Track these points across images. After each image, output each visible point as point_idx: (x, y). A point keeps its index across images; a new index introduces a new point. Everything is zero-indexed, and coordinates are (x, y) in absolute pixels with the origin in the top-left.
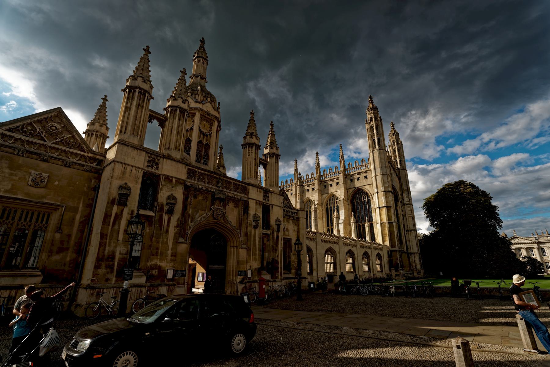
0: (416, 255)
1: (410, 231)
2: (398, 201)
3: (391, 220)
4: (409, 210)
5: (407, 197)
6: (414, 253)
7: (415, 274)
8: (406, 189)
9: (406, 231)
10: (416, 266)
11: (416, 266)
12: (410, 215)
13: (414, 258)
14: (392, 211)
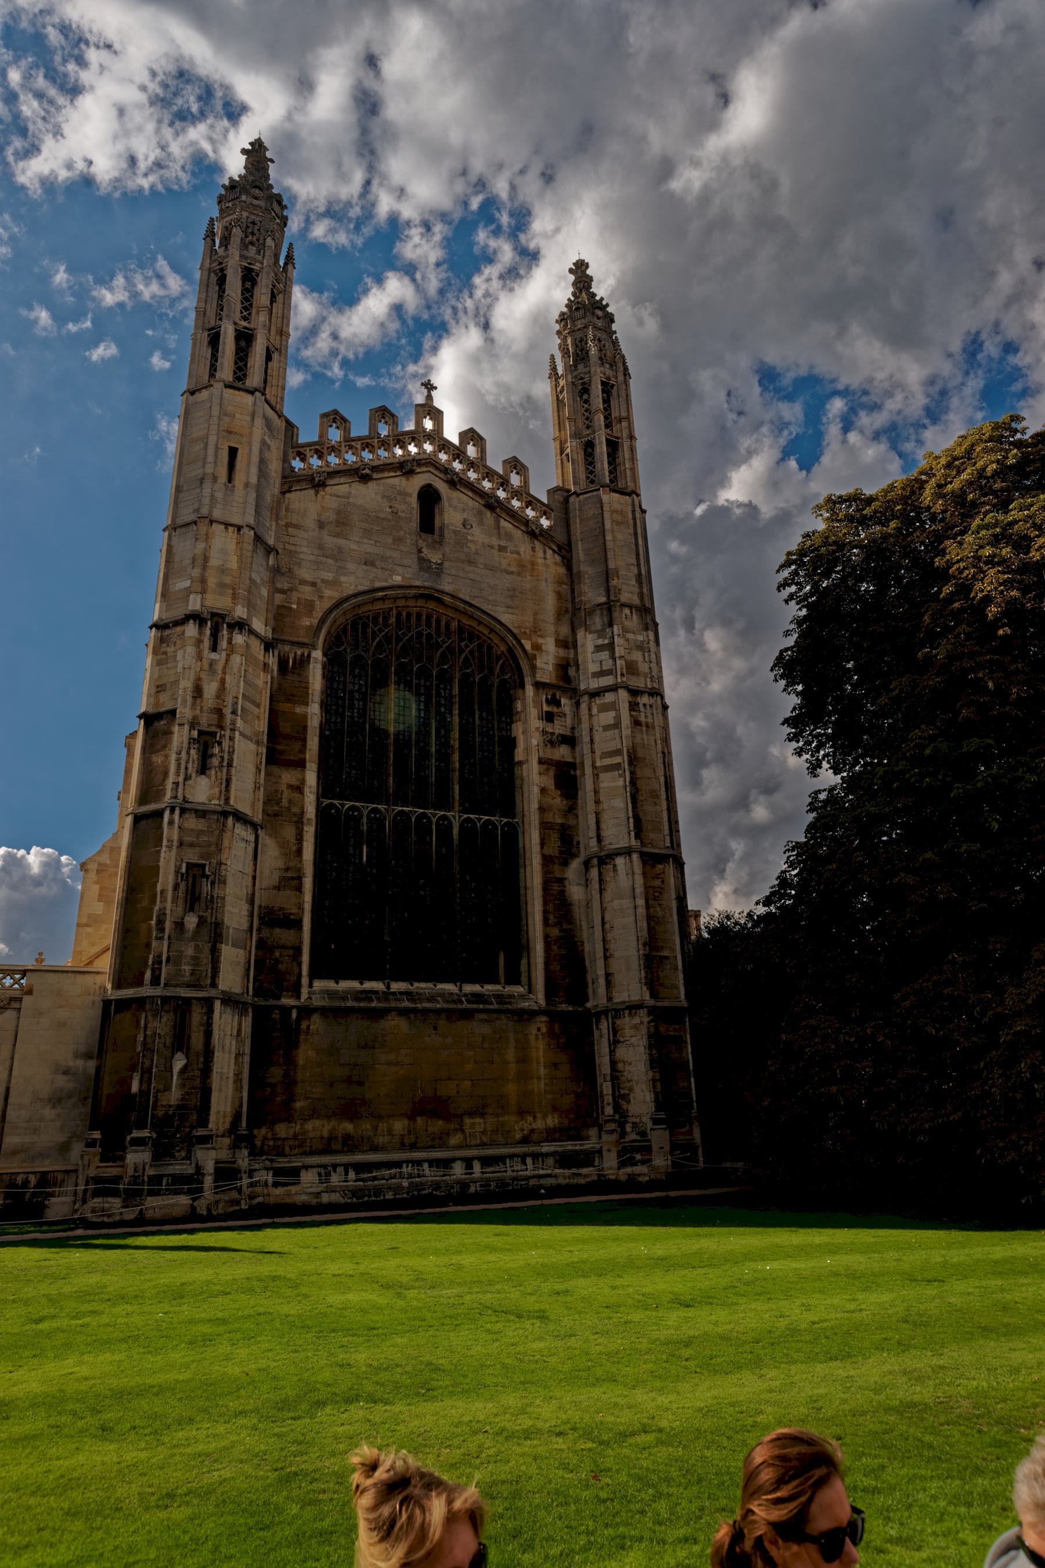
0: (626, 1022)
2: (522, 686)
3: (159, 795)
4: (607, 728)
5: (598, 649)
6: (616, 1012)
7: (610, 1164)
8: (603, 599)
9: (587, 864)
10: (620, 1098)
11: (626, 1098)
13: (614, 1044)
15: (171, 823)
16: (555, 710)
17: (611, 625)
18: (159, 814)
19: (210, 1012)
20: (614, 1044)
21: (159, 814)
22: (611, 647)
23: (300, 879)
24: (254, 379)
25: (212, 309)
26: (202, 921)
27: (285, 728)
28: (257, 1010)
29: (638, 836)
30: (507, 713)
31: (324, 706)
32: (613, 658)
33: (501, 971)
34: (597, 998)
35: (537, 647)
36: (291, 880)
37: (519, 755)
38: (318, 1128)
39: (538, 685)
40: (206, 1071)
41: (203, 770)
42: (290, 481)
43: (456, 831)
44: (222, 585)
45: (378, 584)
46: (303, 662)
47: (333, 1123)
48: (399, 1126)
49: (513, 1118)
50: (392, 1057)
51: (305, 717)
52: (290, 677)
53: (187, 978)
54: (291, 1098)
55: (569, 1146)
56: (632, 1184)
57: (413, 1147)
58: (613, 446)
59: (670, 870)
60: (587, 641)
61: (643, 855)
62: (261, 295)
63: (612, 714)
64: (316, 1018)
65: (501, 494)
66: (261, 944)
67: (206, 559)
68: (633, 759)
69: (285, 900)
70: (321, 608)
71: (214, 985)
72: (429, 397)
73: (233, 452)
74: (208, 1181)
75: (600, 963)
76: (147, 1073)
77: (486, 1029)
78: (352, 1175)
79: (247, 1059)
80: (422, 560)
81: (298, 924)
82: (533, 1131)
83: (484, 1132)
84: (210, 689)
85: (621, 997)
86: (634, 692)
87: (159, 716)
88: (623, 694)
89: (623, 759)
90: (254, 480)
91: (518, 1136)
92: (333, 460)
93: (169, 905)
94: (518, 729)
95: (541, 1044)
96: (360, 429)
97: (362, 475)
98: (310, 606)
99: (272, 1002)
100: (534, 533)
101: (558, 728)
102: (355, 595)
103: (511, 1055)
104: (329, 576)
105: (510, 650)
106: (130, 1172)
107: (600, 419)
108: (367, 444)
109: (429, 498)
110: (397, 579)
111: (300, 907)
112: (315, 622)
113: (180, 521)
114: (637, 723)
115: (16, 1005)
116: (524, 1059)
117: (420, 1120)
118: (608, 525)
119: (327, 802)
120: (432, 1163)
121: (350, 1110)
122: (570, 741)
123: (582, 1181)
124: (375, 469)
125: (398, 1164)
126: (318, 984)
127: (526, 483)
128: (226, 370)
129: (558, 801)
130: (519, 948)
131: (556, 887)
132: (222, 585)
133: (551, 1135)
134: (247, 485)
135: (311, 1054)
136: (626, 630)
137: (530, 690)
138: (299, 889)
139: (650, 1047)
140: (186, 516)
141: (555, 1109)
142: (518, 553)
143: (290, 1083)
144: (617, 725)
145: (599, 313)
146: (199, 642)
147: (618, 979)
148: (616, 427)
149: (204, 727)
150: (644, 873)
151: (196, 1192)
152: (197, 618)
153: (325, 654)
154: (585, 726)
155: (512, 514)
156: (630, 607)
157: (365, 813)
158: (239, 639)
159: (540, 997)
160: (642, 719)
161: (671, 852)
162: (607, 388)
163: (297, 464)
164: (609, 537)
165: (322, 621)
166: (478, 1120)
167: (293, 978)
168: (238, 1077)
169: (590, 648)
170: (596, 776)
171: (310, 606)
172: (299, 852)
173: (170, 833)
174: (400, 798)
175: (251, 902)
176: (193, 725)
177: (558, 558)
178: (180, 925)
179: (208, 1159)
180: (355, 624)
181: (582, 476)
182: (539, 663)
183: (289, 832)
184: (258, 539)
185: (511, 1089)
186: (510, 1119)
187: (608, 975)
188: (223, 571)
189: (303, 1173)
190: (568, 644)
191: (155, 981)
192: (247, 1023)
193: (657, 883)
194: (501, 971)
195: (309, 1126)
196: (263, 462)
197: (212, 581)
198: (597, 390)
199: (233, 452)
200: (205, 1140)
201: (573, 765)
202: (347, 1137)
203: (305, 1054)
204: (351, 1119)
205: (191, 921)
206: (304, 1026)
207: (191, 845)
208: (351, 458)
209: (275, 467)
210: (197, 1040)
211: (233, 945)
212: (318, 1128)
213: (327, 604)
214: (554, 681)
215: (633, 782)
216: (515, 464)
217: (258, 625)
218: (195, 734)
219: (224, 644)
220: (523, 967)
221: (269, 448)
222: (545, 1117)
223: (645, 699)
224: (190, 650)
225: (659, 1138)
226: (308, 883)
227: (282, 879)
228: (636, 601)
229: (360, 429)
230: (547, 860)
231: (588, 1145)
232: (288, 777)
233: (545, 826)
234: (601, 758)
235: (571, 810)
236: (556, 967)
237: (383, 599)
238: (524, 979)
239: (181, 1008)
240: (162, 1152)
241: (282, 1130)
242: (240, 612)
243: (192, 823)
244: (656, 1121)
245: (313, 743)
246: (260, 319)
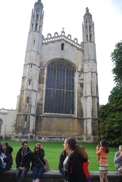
0: (88, 120)
1: (86, 98)
2: (76, 72)
4: (88, 78)
5: (87, 66)
6: (87, 119)
7: (85, 140)
8: (88, 59)
12: (88, 82)
14: (27, 80)
15: (25, 92)
16: (80, 75)
17: (89, 62)
18: (24, 90)
19: (30, 116)
20: (86, 123)
21: (24, 90)
22: (89, 65)
23: (43, 99)
24: (38, 30)
25: (32, 21)
26: (29, 104)
28: (36, 116)
29: (91, 94)
30: (73, 75)
31: (47, 75)
32: (89, 67)
33: (71, 112)
34: (84, 117)
35: (78, 66)
36: (42, 99)
37: (75, 82)
38: (44, 132)
39: (78, 72)
40: (29, 124)
41: (30, 84)
42: (43, 44)
43: (65, 93)
44: (32, 59)
45: (55, 58)
46: (44, 69)
47: (46, 132)
48: (55, 133)
49: (72, 133)
50: (55, 123)
51: (44, 77)
52: (42, 71)
53: (27, 112)
54: (41, 128)
55: (79, 137)
56: (87, 143)
57: (57, 136)
58: (91, 35)
59: (96, 99)
60: (86, 65)
61: (92, 96)
62: (39, 18)
63: (89, 76)
64: (44, 118)
65: (74, 44)
66: (37, 108)
67: (31, 56)
68: (91, 82)
69: (41, 102)
71: (30, 113)
72: (63, 30)
73: (34, 41)
74: (29, 137)
75: (85, 112)
76: (22, 123)
77: (68, 120)
78: (49, 138)
79: (35, 123)
80: (61, 54)
81: (42, 105)
82: (74, 135)
83: (67, 134)
84: (31, 74)
85: (87, 117)
86: (92, 72)
87: (24, 77)
88: (90, 73)
89: (90, 82)
90: (37, 44)
91: (72, 135)
92: (49, 40)
93: (25, 102)
94: (75, 78)
95: (76, 123)
96: (53, 36)
97: (53, 42)
98: (45, 61)
99: (38, 115)
100: (78, 49)
101: (81, 78)
102: (52, 60)
103: (71, 124)
105: (74, 66)
106: (20, 135)
107: (89, 31)
108: (54, 38)
109: (63, 45)
110: (58, 57)
111: (43, 103)
112: (46, 64)
113: (28, 51)
114: (92, 77)
115: (7, 114)
116: (73, 125)
117: (58, 132)
118: (89, 47)
119: (47, 89)
120: (59, 138)
121: (49, 130)
122: (83, 80)
123: (81, 142)
124: (55, 41)
125: (55, 138)
126: (45, 113)
127: (77, 41)
128: (34, 30)
129: (80, 88)
130: (73, 109)
131: (79, 101)
132: (32, 59)
133: (77, 135)
134: (36, 45)
135: (44, 122)
136: (91, 63)
137: (77, 72)
138: (43, 100)
139: (91, 124)
140: (28, 50)
141: (78, 132)
143: (41, 126)
144: (89, 77)
145: (89, 15)
146: (29, 67)
147: (87, 114)
148: (91, 32)
149: (30, 79)
150: (92, 99)
151: (28, 139)
152: (29, 64)
154: (85, 77)
155: (75, 46)
156: (92, 60)
157: (56, 91)
158: (35, 66)
159: (76, 116)
160: (93, 76)
161: (96, 96)
162: (90, 26)
163: (44, 41)
164: (89, 49)
165: (47, 63)
166: (66, 133)
167: (42, 112)
168: (33, 125)
169: (86, 66)
170: (86, 85)
172: (43, 95)
173: (25, 93)
174: (57, 88)
176: (28, 78)
177: (82, 53)
178: (26, 105)
179: (29, 135)
180: (52, 64)
181: (86, 40)
182: (78, 68)
183: (41, 93)
184: (38, 52)
185: (71, 129)
186: (71, 133)
187: (86, 114)
188: (33, 57)
189: (42, 138)
190: (83, 65)
191: (23, 112)
193: (94, 101)
194: (71, 112)
195: (43, 132)
196: (39, 42)
197: (31, 59)
198: (88, 27)
199: (34, 41)
200: (29, 132)
201: (83, 83)
202: (48, 134)
203: (43, 122)
204: (49, 131)
205: (28, 104)
206: (43, 119)
207: (28, 94)
208: (51, 40)
209: (40, 42)
210: (28, 120)
211: (33, 108)
212: (44, 132)
213: (48, 61)
214: (81, 71)
215: (91, 86)
216: (76, 39)
217: (38, 65)
218: (28, 80)
219: (32, 67)
220: (74, 112)
221: (40, 40)
222: (76, 133)
223: (94, 73)
224: (28, 68)
225: (92, 137)
226: (44, 100)
227: (40, 99)
228: (93, 59)
229: (53, 36)
230: (78, 97)
231: (82, 137)
232: (41, 85)
233: (78, 92)
234: (87, 82)
235: (82, 90)
236: (79, 112)
237: (56, 60)
238: (74, 114)
239: (26, 115)
240: (23, 133)
241: (40, 132)
242: (35, 63)
243: (28, 91)
244: (92, 134)
246: (39, 22)
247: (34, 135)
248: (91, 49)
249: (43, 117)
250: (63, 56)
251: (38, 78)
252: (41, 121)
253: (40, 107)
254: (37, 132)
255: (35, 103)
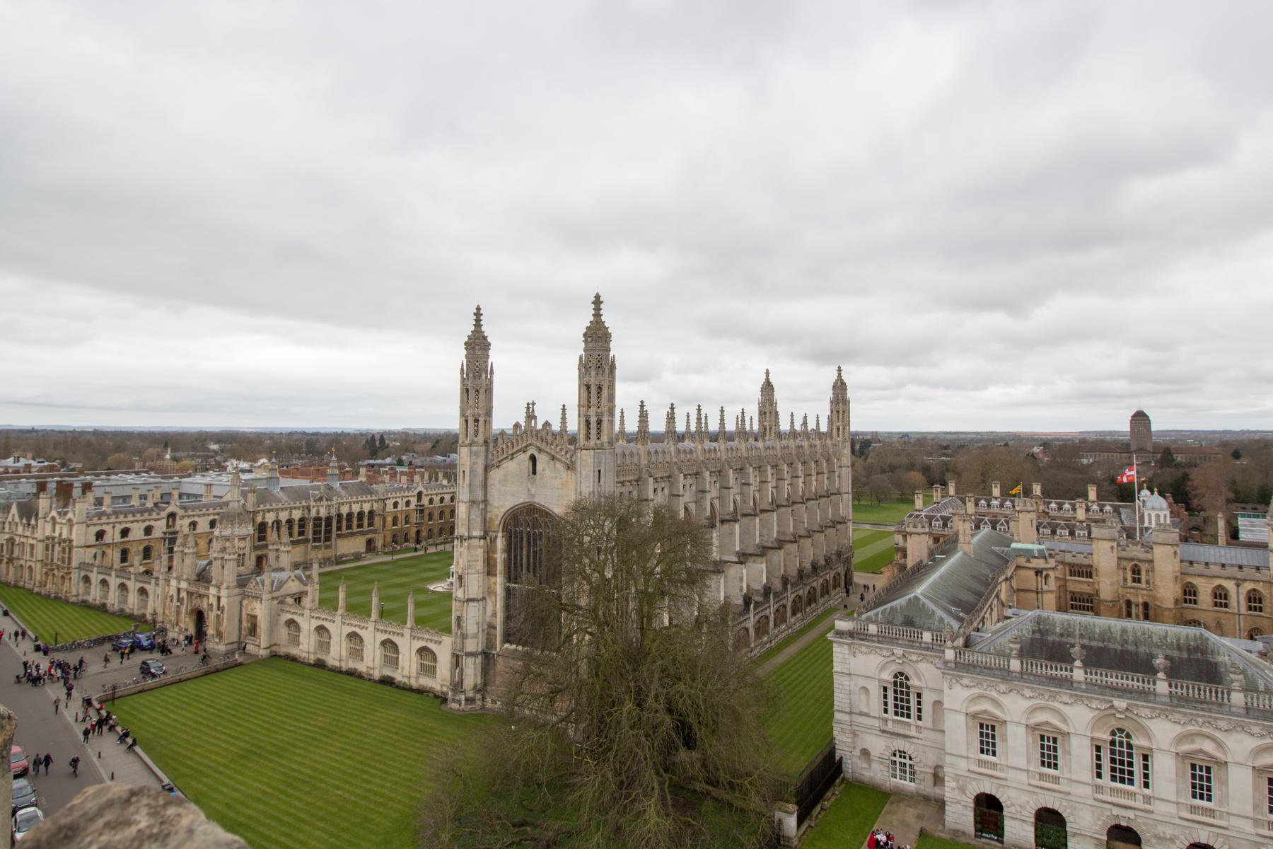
27: (492, 562)
31: (504, 551)
36: (494, 615)
45: (516, 503)
46: (496, 537)
66: (488, 634)
69: (492, 620)
70: (500, 516)
74: (463, 703)
80: (529, 490)
98: (497, 516)
104: (502, 503)
109: (533, 458)
110: (521, 500)
126: (507, 645)
138: (496, 617)
142: (561, 478)
151: (460, 705)
153: (503, 531)
168: (475, 675)
171: (497, 516)
175: (478, 624)
178: (457, 633)
192: (479, 659)
205: (459, 633)
232: (493, 579)
245: (500, 567)
247: (479, 696)
248: (584, 473)
249: (498, 655)
250: (533, 496)
251: (480, 565)
252: (495, 665)
253: (492, 631)
254: (489, 688)
255: (476, 626)
